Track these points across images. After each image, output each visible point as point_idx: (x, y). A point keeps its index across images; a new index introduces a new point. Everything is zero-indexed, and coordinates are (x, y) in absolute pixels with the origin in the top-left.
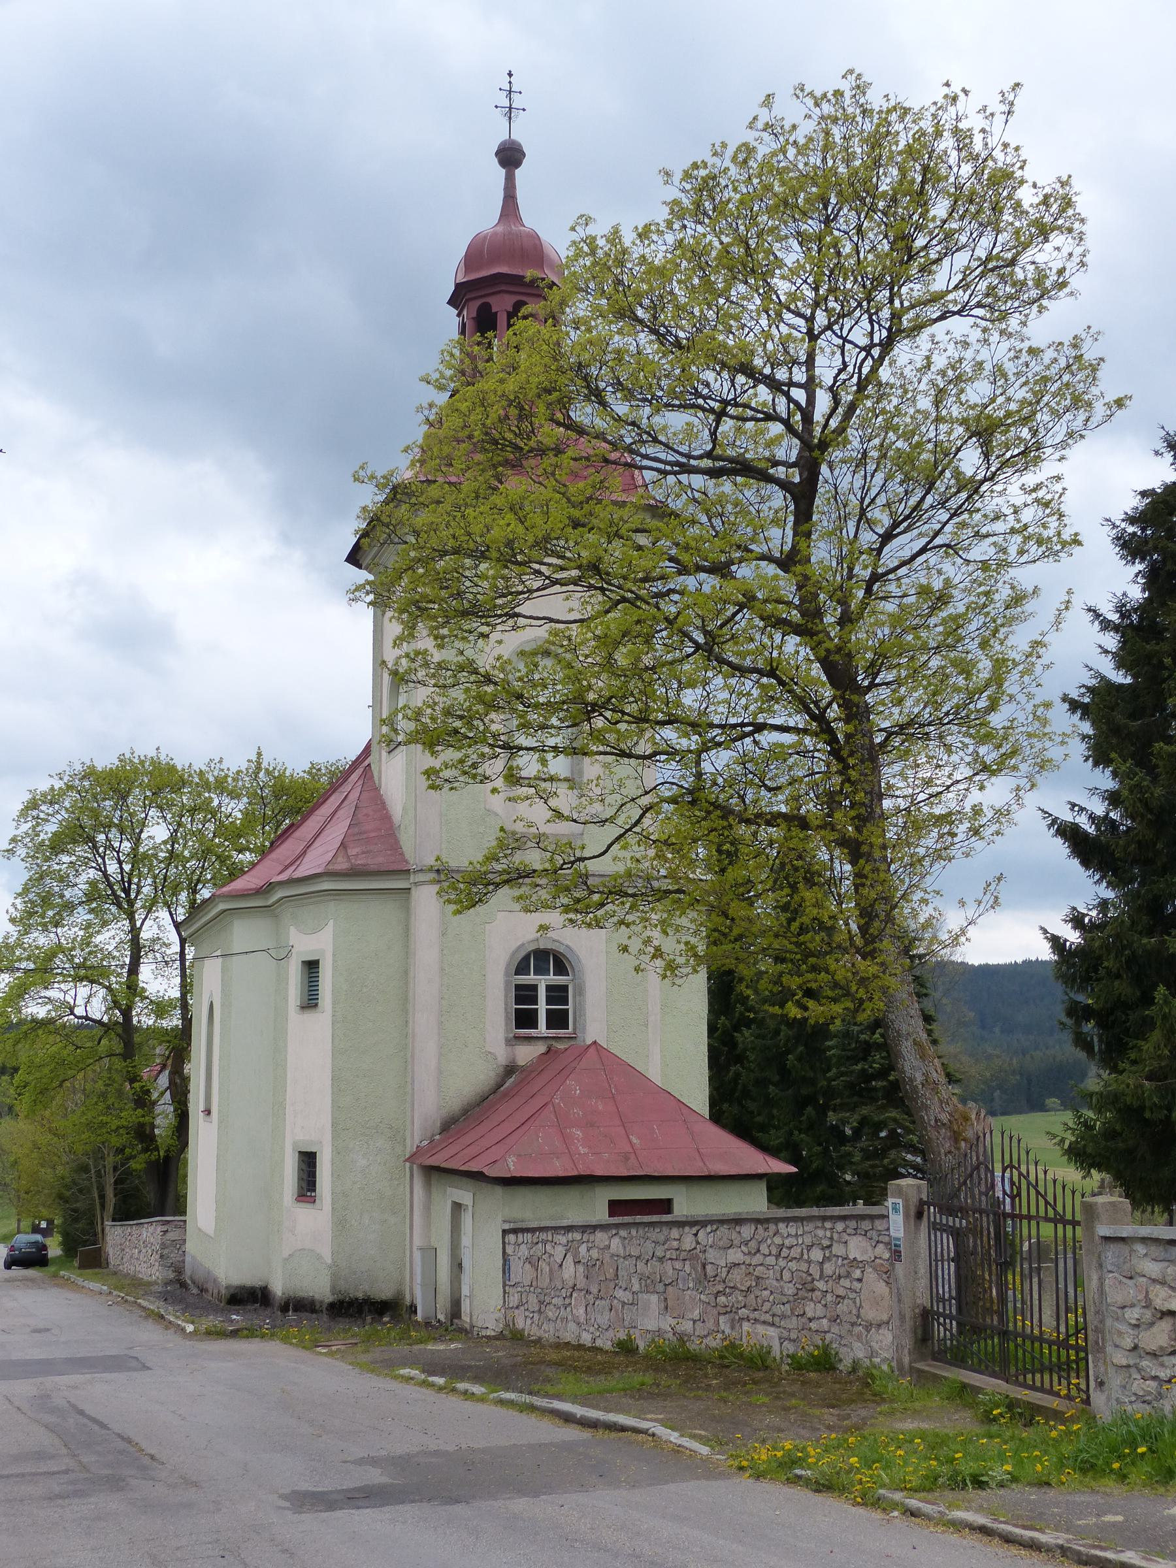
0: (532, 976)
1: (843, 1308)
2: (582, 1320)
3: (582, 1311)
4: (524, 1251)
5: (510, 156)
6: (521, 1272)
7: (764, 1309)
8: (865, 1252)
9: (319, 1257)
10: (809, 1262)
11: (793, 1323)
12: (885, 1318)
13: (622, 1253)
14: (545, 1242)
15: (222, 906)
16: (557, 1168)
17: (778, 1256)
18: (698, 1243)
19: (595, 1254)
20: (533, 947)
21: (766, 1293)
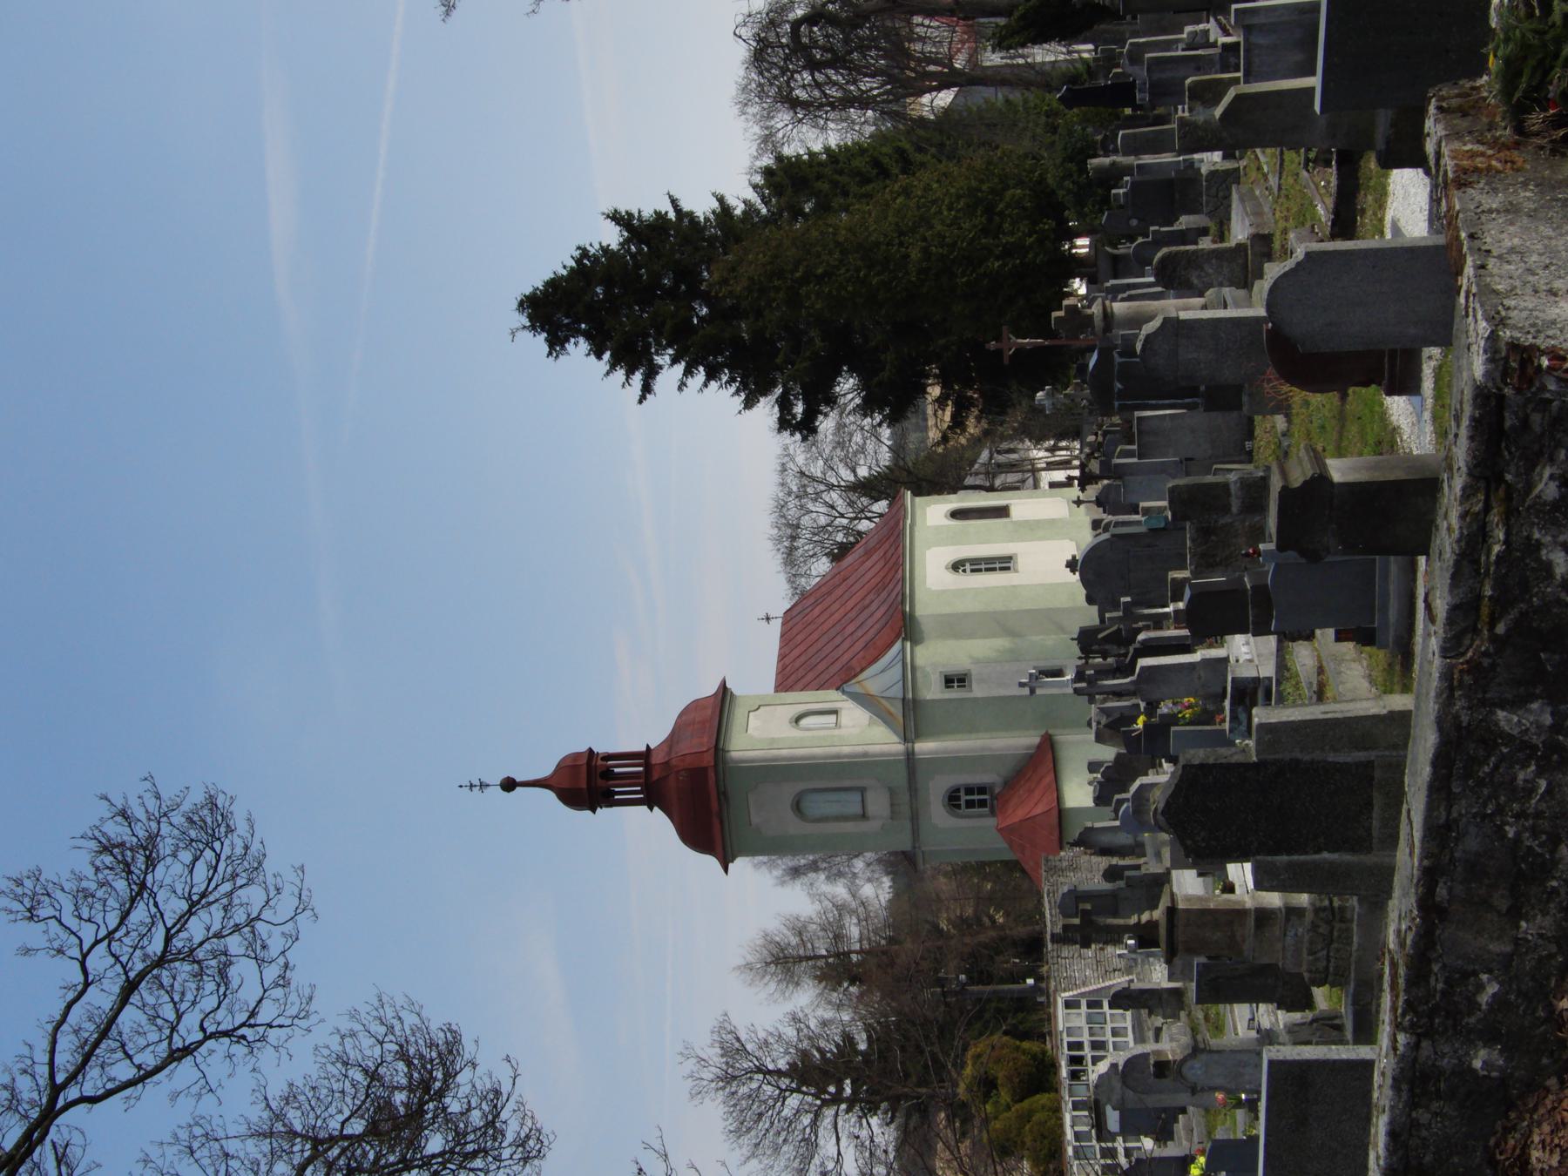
5: (509, 785)
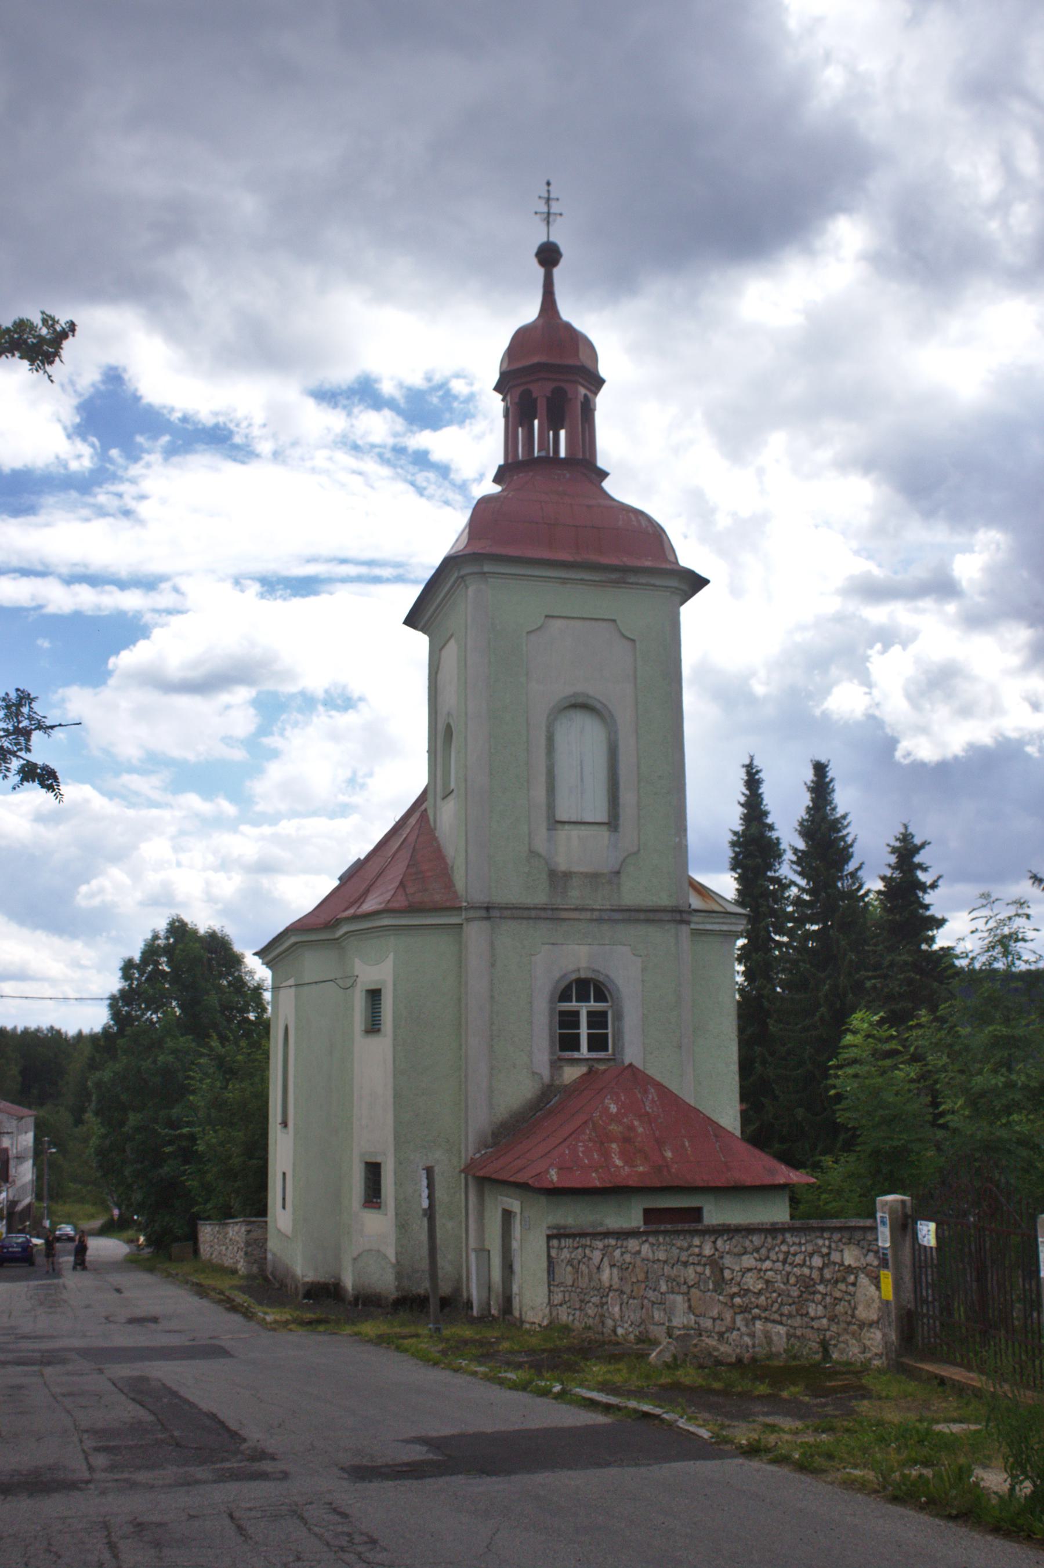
0: (574, 1003)
1: (840, 1308)
2: (617, 1316)
3: (617, 1309)
4: (565, 1254)
6: (565, 1274)
7: (774, 1309)
8: (858, 1259)
9: (385, 1257)
10: (811, 1268)
11: (797, 1321)
12: (875, 1317)
13: (650, 1256)
14: (584, 1247)
15: (293, 940)
16: (595, 1180)
17: (784, 1262)
18: (716, 1250)
19: (628, 1258)
20: (574, 976)
21: (775, 1295)
